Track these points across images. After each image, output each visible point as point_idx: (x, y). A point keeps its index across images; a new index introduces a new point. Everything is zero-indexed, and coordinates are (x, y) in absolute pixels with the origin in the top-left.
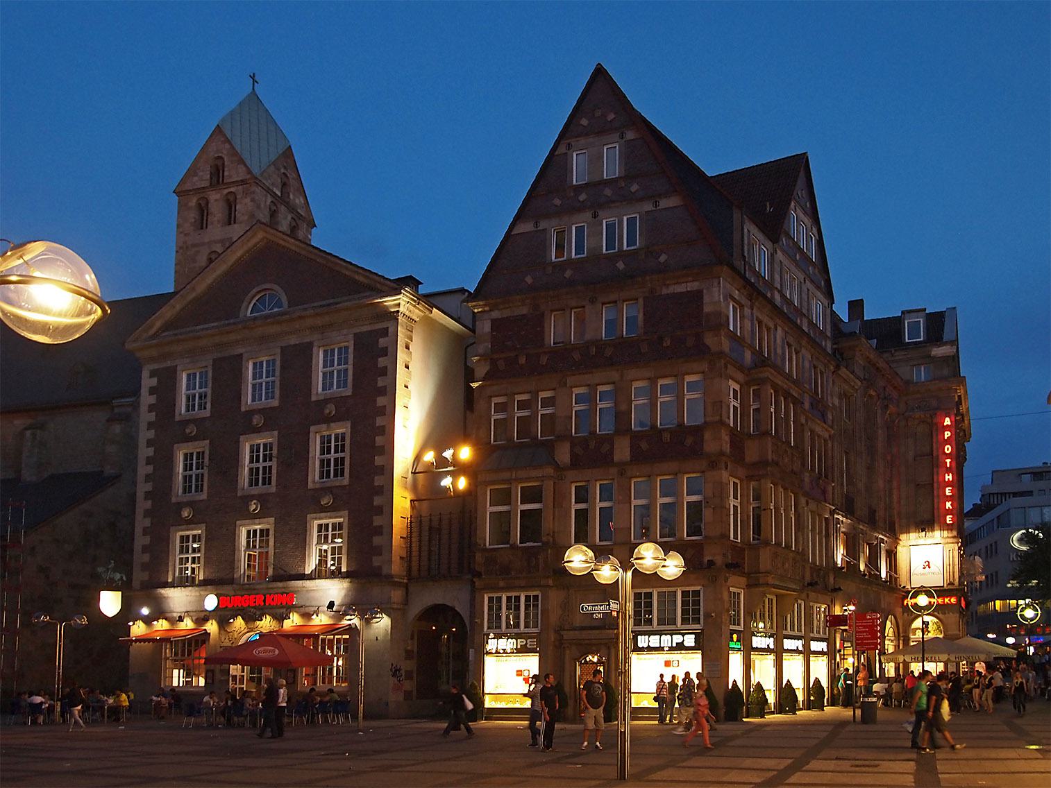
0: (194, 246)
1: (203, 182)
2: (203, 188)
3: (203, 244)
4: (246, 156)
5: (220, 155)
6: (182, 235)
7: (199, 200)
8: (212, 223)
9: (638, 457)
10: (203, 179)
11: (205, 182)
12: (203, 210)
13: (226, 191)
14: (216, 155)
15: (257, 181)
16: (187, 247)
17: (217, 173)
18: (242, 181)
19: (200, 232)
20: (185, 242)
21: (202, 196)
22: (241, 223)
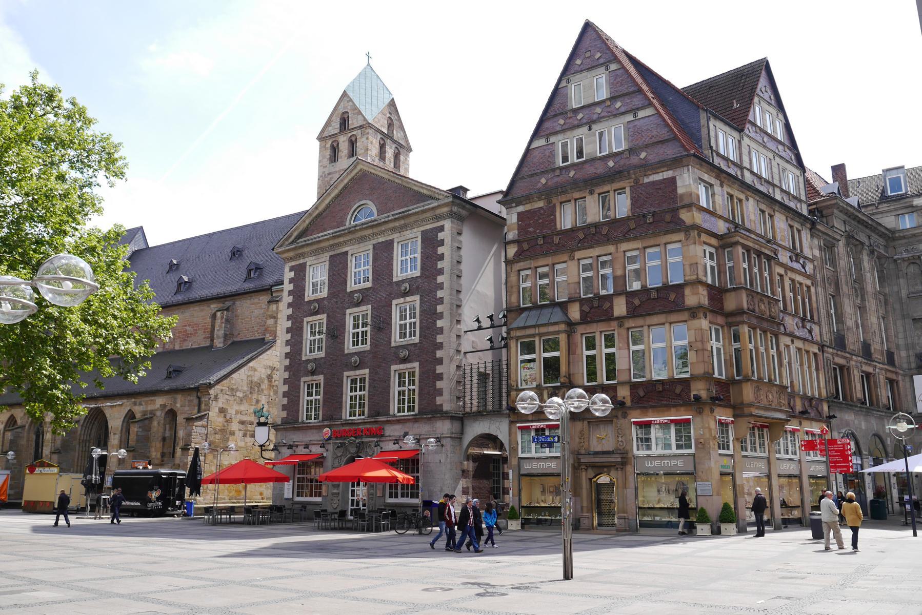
2: (336, 134)
4: (362, 109)
5: (346, 110)
7: (332, 142)
8: (341, 158)
10: (335, 127)
12: (335, 149)
15: (370, 126)
16: (325, 175)
17: (344, 122)
18: (360, 126)
19: (334, 164)
20: (324, 172)
21: (334, 139)
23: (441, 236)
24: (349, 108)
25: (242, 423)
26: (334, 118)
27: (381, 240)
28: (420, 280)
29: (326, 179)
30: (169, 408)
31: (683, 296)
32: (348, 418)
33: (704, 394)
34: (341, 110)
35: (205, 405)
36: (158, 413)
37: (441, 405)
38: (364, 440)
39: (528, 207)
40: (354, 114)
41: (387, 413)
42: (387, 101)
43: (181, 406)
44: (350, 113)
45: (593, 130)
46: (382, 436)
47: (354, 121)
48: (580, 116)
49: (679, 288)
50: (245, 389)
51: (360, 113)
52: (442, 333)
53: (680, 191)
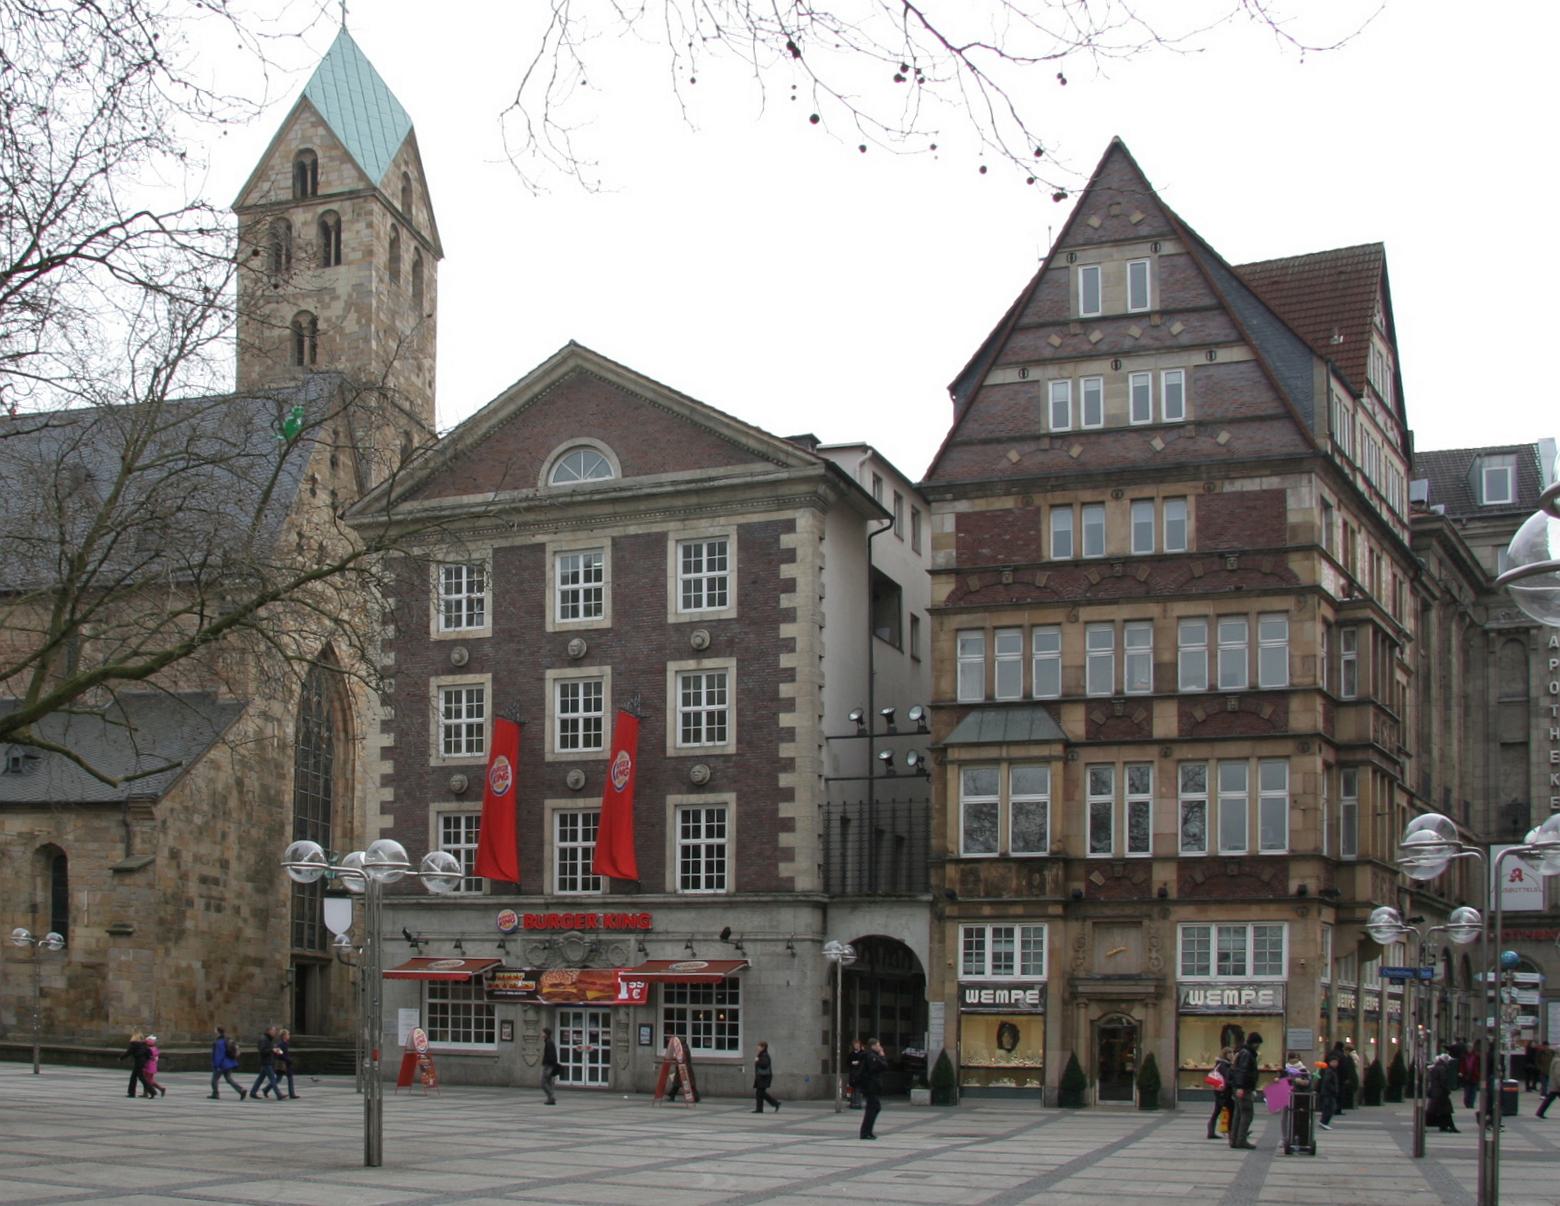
4: (353, 148)
5: (309, 146)
9: (1191, 734)
10: (283, 186)
13: (321, 209)
14: (302, 147)
15: (372, 192)
17: (306, 172)
18: (351, 192)
22: (350, 263)
23: (787, 540)
24: (317, 141)
25: (204, 880)
26: (276, 161)
27: (633, 530)
28: (736, 628)
30: (46, 842)
31: (1286, 712)
32: (558, 892)
33: (1313, 886)
34: (295, 144)
35: (144, 841)
36: (17, 851)
37: (791, 880)
38: (603, 937)
39: (980, 505)
40: (332, 159)
41: (660, 888)
42: (403, 135)
43: (76, 840)
44: (320, 154)
45: (1122, 371)
46: (647, 931)
47: (333, 176)
48: (1095, 336)
49: (1281, 695)
50: (205, 807)
51: (347, 157)
52: (793, 740)
53: (1293, 518)
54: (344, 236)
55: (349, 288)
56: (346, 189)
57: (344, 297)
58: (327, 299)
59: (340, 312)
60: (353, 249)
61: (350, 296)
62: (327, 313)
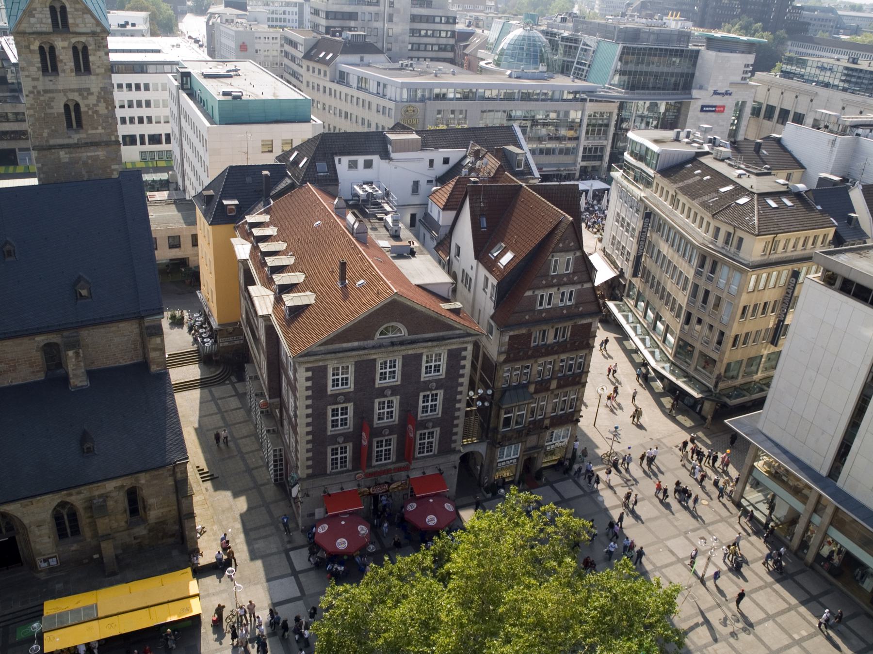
0: (46, 91)
1: (42, 25)
3: (58, 91)
6: (30, 79)
8: (64, 71)
11: (45, 26)
23: (464, 353)
27: (410, 352)
29: (42, 98)
39: (516, 332)
40: (76, 10)
44: (67, 5)
54: (91, 58)
55: (99, 89)
56: (89, 30)
57: (96, 94)
58: (85, 94)
59: (95, 102)
60: (99, 67)
61: (100, 93)
62: (86, 102)
